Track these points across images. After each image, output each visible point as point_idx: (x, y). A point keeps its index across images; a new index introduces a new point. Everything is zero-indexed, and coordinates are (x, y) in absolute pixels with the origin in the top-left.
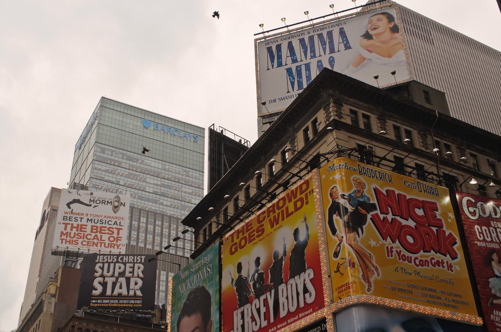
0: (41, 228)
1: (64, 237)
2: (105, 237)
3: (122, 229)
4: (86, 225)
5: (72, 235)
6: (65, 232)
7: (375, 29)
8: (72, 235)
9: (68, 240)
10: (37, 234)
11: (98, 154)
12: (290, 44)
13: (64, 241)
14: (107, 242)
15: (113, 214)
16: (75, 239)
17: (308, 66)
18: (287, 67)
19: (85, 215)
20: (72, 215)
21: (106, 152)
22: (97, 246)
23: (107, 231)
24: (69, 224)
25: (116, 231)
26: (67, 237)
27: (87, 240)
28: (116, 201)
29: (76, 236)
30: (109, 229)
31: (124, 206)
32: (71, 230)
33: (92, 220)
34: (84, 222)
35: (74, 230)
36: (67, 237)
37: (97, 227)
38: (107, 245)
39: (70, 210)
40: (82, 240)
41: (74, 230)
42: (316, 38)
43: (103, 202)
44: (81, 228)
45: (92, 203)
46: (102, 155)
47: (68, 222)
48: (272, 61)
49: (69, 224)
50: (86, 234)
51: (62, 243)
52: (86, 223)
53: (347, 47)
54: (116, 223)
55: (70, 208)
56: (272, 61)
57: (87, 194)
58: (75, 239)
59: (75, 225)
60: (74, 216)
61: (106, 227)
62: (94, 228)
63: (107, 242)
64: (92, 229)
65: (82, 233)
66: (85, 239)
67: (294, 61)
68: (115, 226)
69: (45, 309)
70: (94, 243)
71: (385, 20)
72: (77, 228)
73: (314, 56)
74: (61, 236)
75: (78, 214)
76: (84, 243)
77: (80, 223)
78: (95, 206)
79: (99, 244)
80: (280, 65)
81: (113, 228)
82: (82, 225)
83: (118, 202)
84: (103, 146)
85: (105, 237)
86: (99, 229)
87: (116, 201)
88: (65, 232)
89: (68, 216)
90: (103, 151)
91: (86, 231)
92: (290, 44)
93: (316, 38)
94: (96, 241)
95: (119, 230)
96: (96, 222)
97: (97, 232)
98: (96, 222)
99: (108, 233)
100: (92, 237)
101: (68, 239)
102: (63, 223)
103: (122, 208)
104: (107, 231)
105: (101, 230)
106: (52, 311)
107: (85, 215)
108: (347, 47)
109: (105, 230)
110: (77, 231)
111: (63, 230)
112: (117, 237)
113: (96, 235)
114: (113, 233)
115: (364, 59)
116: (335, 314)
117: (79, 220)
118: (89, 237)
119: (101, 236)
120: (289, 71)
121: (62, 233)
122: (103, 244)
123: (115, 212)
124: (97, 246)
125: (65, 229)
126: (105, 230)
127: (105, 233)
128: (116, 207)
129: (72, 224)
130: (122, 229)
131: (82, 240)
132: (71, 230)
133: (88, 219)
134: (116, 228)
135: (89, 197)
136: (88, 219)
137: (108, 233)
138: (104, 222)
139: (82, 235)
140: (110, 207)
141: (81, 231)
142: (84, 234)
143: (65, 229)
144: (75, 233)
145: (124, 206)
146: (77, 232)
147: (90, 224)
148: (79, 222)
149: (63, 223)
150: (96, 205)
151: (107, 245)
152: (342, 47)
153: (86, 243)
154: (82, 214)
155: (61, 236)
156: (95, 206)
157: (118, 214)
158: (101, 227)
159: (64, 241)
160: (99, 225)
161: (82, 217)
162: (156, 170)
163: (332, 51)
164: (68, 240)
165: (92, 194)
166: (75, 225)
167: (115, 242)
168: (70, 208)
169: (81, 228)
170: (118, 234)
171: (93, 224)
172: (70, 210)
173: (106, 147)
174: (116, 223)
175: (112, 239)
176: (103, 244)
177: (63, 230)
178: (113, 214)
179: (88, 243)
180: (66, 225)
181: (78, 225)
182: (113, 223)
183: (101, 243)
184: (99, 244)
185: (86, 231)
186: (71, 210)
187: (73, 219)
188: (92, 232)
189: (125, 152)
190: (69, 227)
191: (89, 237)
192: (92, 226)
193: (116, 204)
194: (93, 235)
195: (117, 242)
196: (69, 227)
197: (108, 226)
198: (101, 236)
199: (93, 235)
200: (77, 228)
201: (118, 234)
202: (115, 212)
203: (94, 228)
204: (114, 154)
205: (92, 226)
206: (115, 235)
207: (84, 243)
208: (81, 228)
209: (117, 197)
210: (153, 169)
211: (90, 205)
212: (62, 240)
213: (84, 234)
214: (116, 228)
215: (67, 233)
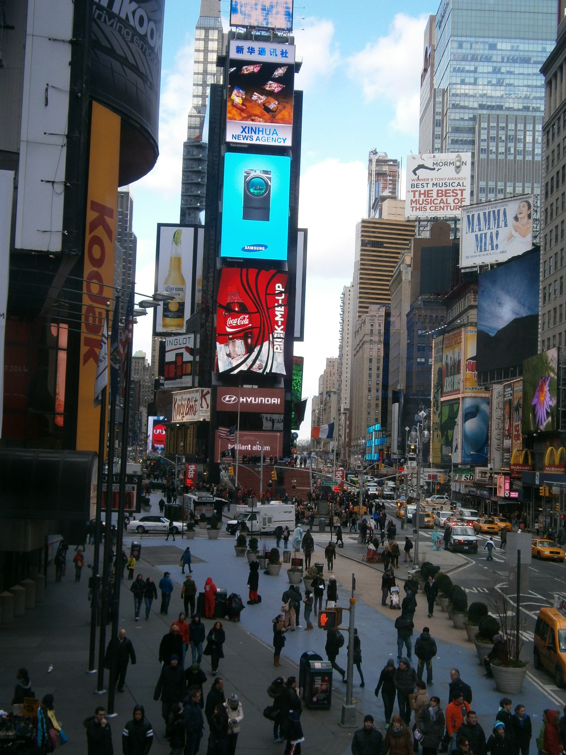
0: (425, 70)
1: (414, 205)
2: (450, 200)
3: (465, 190)
4: (432, 190)
5: (421, 202)
6: (414, 200)
7: (521, 213)
8: (421, 202)
9: (418, 207)
10: (423, 77)
11: (455, 51)
12: (479, 214)
13: (414, 209)
14: (452, 205)
15: (455, 175)
16: (423, 205)
17: (486, 234)
18: (476, 233)
19: (430, 180)
20: (418, 182)
21: (464, 45)
22: (443, 209)
23: (451, 194)
24: (417, 191)
25: (459, 192)
26: (416, 204)
27: (434, 205)
28: (457, 161)
29: (425, 202)
30: (453, 192)
31: (466, 164)
32: (420, 197)
33: (437, 184)
34: (430, 187)
35: (422, 196)
36: (416, 204)
37: (442, 191)
38: (452, 208)
39: (416, 177)
40: (429, 206)
41: (422, 196)
42: (492, 213)
43: (445, 164)
44: (428, 194)
45: (435, 166)
46: (459, 51)
47: (415, 189)
48: (469, 228)
49: (417, 191)
50: (433, 199)
51: (413, 211)
52: (432, 189)
53: (506, 225)
54: (459, 184)
55: (416, 174)
56: (469, 228)
57: (430, 158)
58: (423, 205)
59: (422, 192)
60: (422, 182)
61: (450, 190)
62: (440, 192)
63: (452, 205)
64: (438, 193)
65: (430, 198)
66: (433, 205)
67: (480, 230)
68: (459, 187)
69: (403, 278)
70: (440, 207)
71: (527, 207)
72: (424, 194)
73: (489, 229)
74: (411, 204)
75: (424, 180)
76: (432, 208)
77: (427, 189)
78: (439, 169)
79: (445, 208)
80: (473, 231)
81: (457, 190)
82: (428, 191)
83: (460, 161)
84: (460, 39)
85: (450, 200)
86: (444, 193)
87: (457, 161)
88: (414, 200)
89: (415, 183)
90: (460, 46)
91: (432, 197)
92: (479, 214)
93: (492, 213)
94: (442, 205)
95: (462, 191)
96: (441, 185)
97: (442, 196)
98: (441, 185)
99: (453, 196)
100: (438, 202)
101: (418, 206)
102: (412, 191)
103: (463, 167)
104: (451, 194)
105: (446, 193)
106: (410, 279)
107: (430, 180)
108: (506, 225)
109: (450, 193)
110: (425, 197)
111: (412, 198)
112: (461, 199)
113: (442, 199)
114: (457, 194)
115: (512, 236)
116: (463, 398)
117: (425, 185)
118: (436, 202)
119: (447, 199)
120: (476, 236)
121: (412, 200)
122: (449, 208)
123: (458, 173)
124: (443, 209)
125: (414, 197)
126: (450, 193)
127: (450, 196)
128: (458, 167)
129: (420, 191)
130: (465, 190)
131: (429, 206)
132: (420, 197)
133: (433, 184)
134: (459, 190)
135: (432, 161)
136: (433, 184)
137: (453, 196)
138: (448, 184)
139: (429, 201)
140: (452, 168)
141: (428, 196)
142: (431, 200)
143: (414, 197)
144: (423, 200)
145: (466, 164)
146: (425, 199)
147: (435, 189)
148: (425, 188)
149: (412, 191)
150: (440, 167)
151: (452, 208)
152: (503, 225)
153: (433, 208)
154: (428, 180)
155: (411, 204)
156: (439, 169)
157: (460, 175)
158: (446, 190)
159: (414, 209)
160: (443, 188)
161: (427, 182)
162: (526, 54)
163: (498, 227)
164: (418, 207)
165: (434, 157)
166: (422, 192)
167: (459, 204)
168: (416, 174)
169: (427, 193)
170: (462, 195)
171: (439, 188)
172: (416, 177)
173: (464, 39)
174: (459, 184)
175: (456, 201)
176: (449, 208)
177: (412, 198)
178: (455, 175)
179: (435, 208)
180: (414, 192)
181: (425, 191)
182: (456, 184)
183: (447, 207)
184: (445, 208)
185: (432, 197)
186: (417, 176)
187: (420, 186)
188: (438, 196)
189: (486, 40)
190: (417, 194)
191: (436, 202)
192: (438, 191)
193: (458, 164)
194: (440, 199)
195: (461, 203)
196: (417, 194)
197: (452, 188)
198: (447, 199)
199: (440, 199)
200: (424, 194)
201: (462, 195)
202: (458, 173)
203: (440, 192)
204: (474, 45)
205: (438, 191)
206: (459, 197)
207: (432, 208)
208: (427, 193)
209: (458, 156)
210: (521, 53)
211: (434, 169)
212: (413, 207)
213: (431, 200)
214: (459, 190)
215: (416, 200)
